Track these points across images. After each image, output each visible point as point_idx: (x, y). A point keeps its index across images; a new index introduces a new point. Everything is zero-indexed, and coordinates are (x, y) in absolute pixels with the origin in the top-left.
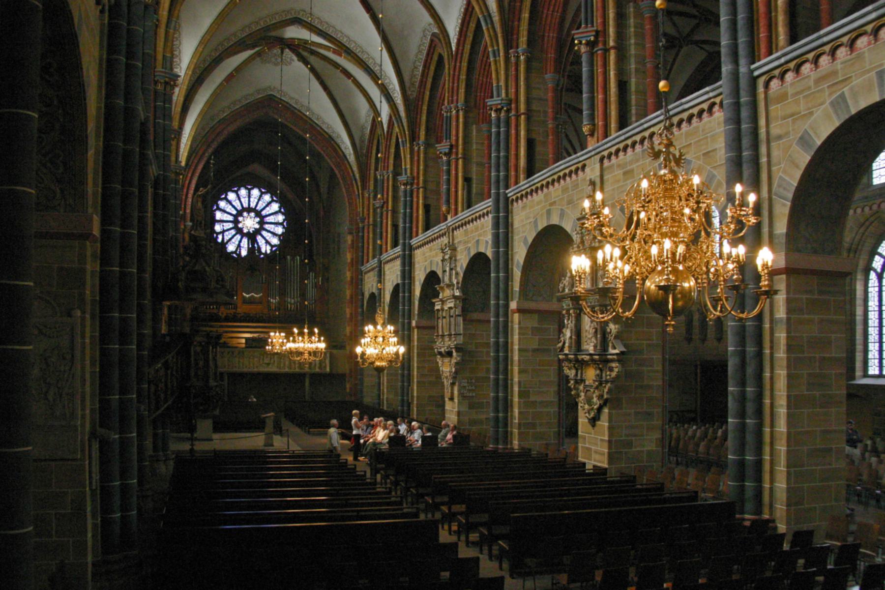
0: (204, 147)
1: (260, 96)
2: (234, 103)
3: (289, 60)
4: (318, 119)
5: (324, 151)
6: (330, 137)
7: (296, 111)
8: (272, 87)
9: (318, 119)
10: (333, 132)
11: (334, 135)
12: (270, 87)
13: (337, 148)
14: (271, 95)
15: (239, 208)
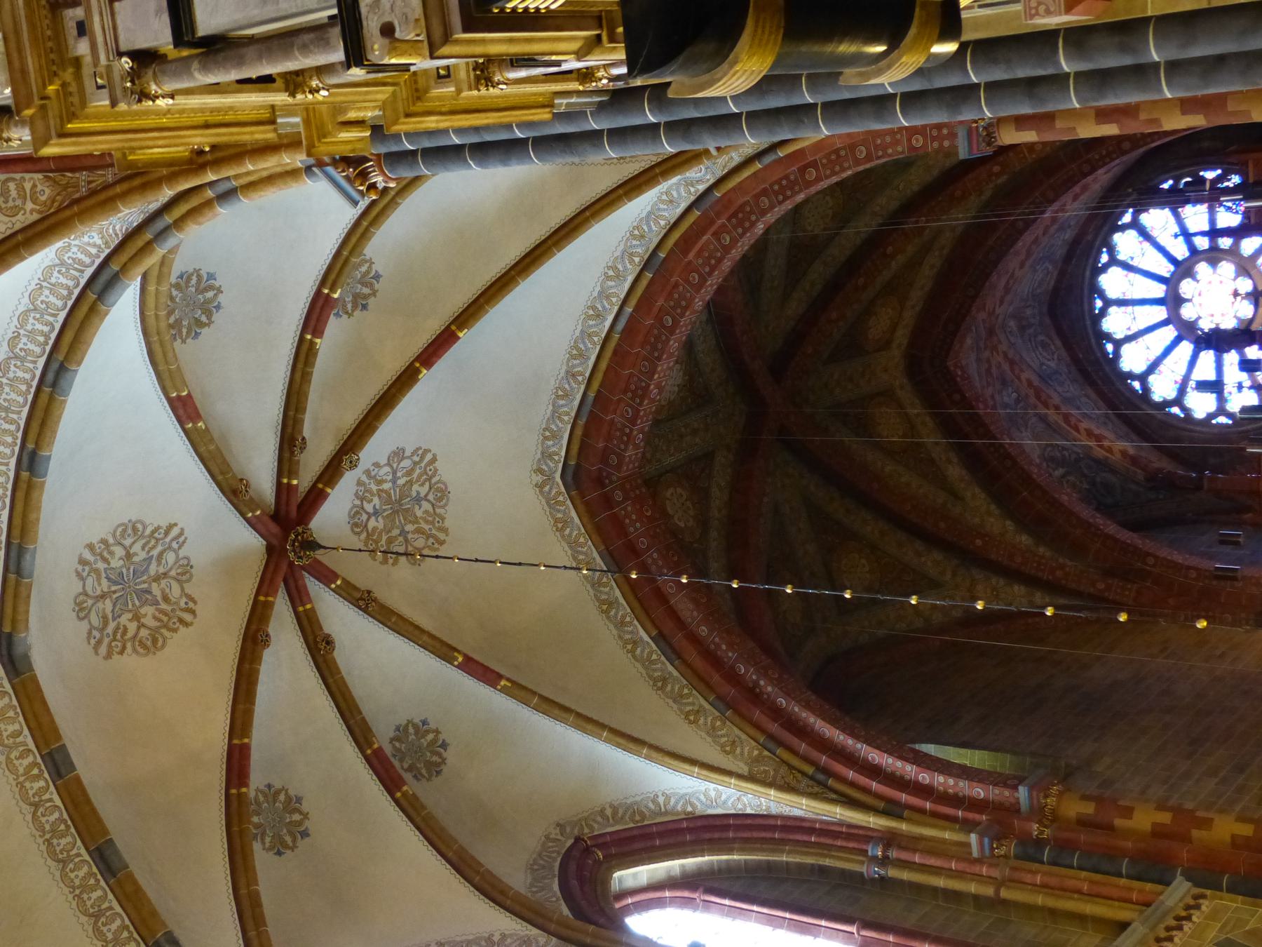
0: (757, 715)
1: (573, 514)
2: (607, 606)
3: (406, 463)
4: (599, 316)
5: (703, 280)
6: (646, 266)
7: (592, 395)
8: (539, 478)
9: (599, 316)
10: (628, 254)
11: (641, 251)
12: (540, 486)
13: (676, 235)
14: (562, 477)
15: (1170, 333)
